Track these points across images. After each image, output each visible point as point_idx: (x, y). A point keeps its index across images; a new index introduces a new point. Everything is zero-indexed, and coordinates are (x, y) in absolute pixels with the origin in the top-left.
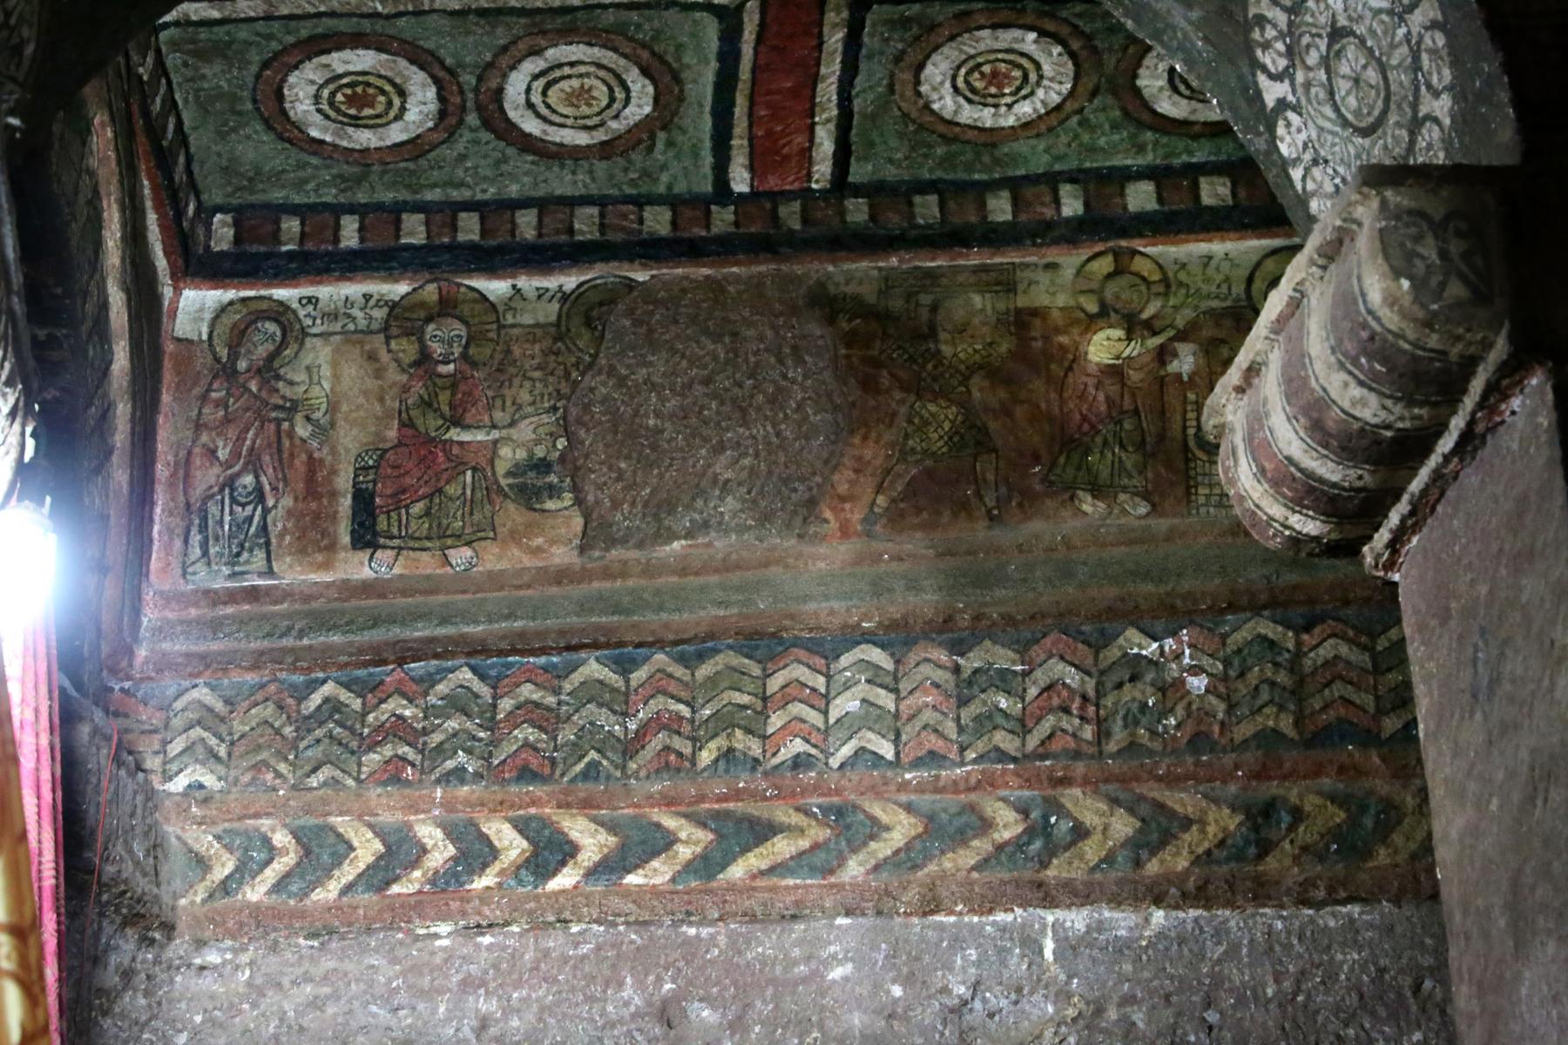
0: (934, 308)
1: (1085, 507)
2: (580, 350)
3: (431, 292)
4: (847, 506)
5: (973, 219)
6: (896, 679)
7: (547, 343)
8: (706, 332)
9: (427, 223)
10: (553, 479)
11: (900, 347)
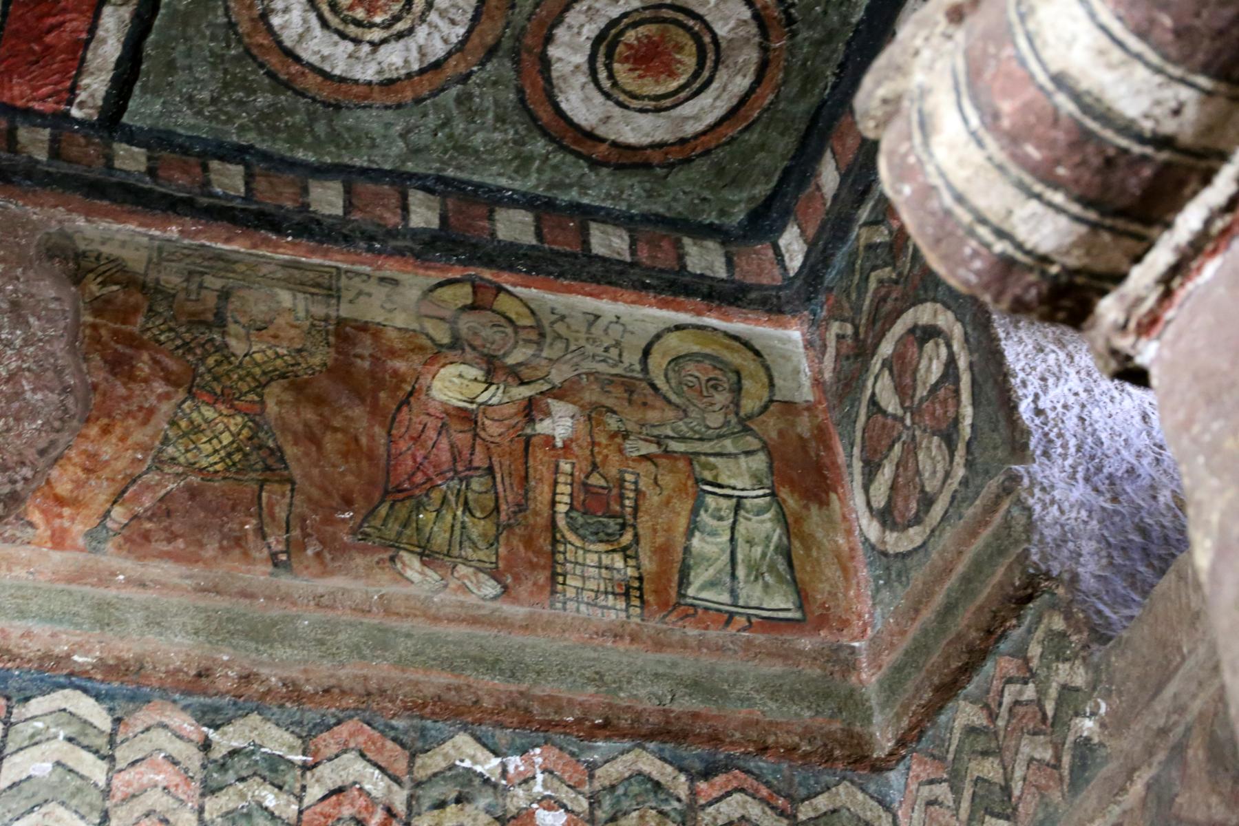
0: (225, 295)
1: (409, 573)
4: (67, 511)
5: (289, 205)
6: (112, 743)
11: (171, 330)
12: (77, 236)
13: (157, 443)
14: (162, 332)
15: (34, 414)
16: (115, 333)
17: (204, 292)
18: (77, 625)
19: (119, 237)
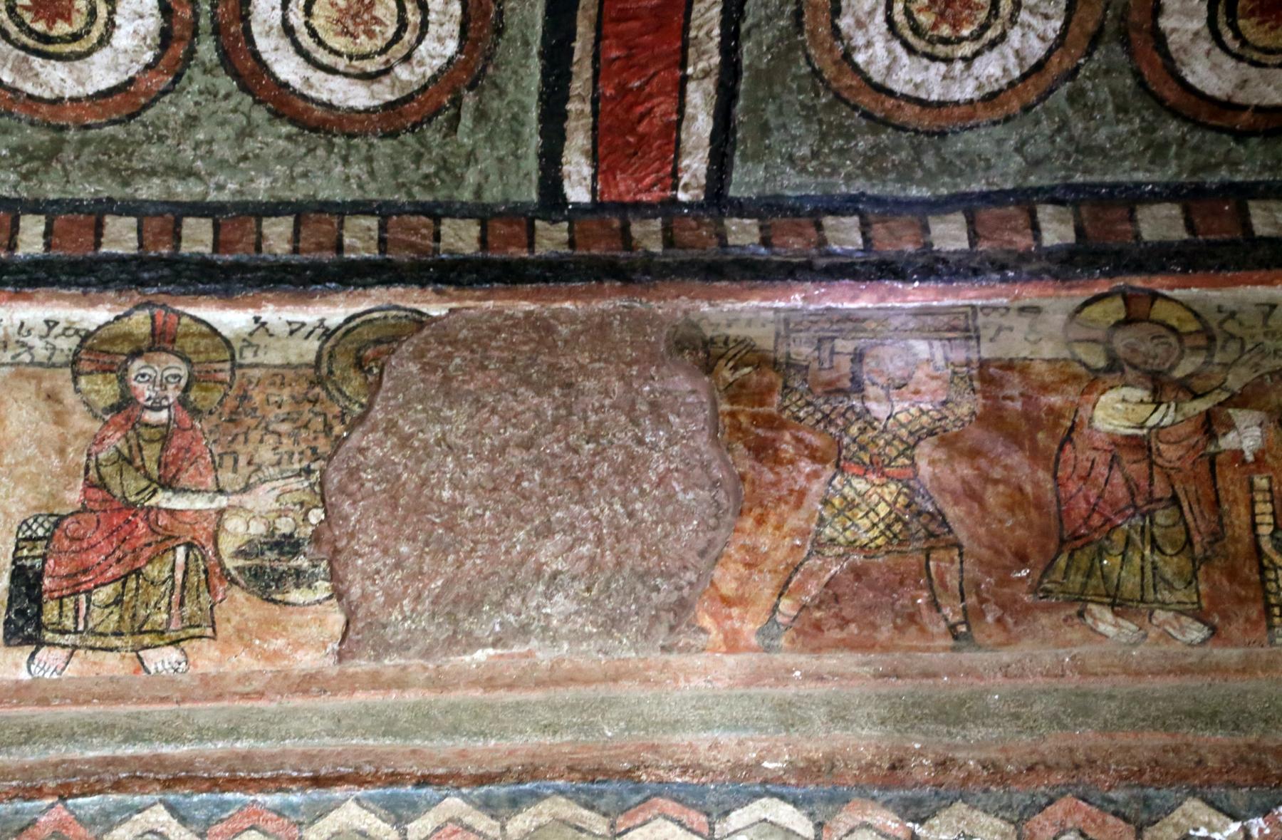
0: (858, 357)
2: (349, 399)
3: (140, 323)
4: (735, 611)
7: (300, 389)
8: (526, 381)
9: (140, 231)
10: (302, 562)
11: (808, 404)
12: (703, 324)
13: (813, 526)
14: (801, 408)
15: (689, 514)
16: (754, 417)
17: (836, 358)
18: (761, 730)
19: (745, 316)
